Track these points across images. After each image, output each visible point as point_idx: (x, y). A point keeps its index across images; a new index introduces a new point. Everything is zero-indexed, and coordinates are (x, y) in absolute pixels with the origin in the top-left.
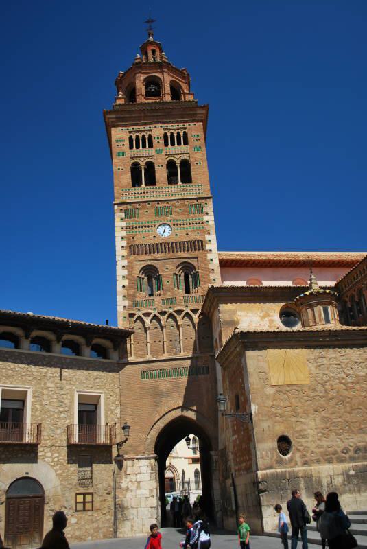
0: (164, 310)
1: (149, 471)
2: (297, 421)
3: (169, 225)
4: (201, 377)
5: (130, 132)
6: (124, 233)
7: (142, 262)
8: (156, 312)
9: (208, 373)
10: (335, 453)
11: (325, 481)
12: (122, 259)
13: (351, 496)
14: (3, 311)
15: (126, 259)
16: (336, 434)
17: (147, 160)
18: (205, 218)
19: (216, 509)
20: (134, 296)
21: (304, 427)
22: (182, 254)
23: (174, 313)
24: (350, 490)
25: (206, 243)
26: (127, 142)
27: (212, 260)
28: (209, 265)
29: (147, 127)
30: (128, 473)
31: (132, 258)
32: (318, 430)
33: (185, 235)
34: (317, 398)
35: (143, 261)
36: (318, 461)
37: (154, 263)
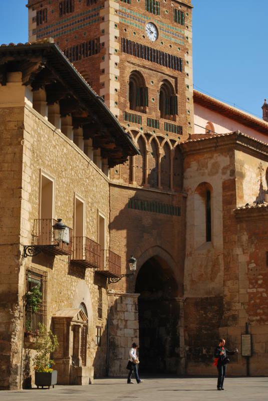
0: (149, 132)
1: (134, 311)
3: (157, 29)
4: (174, 217)
7: (133, 66)
8: (142, 132)
9: (179, 215)
12: (115, 54)
15: (119, 55)
18: (188, 33)
19: (181, 356)
22: (167, 70)
23: (156, 138)
28: (186, 92)
30: (118, 309)
31: (124, 55)
33: (168, 45)
35: (132, 63)
37: (142, 70)
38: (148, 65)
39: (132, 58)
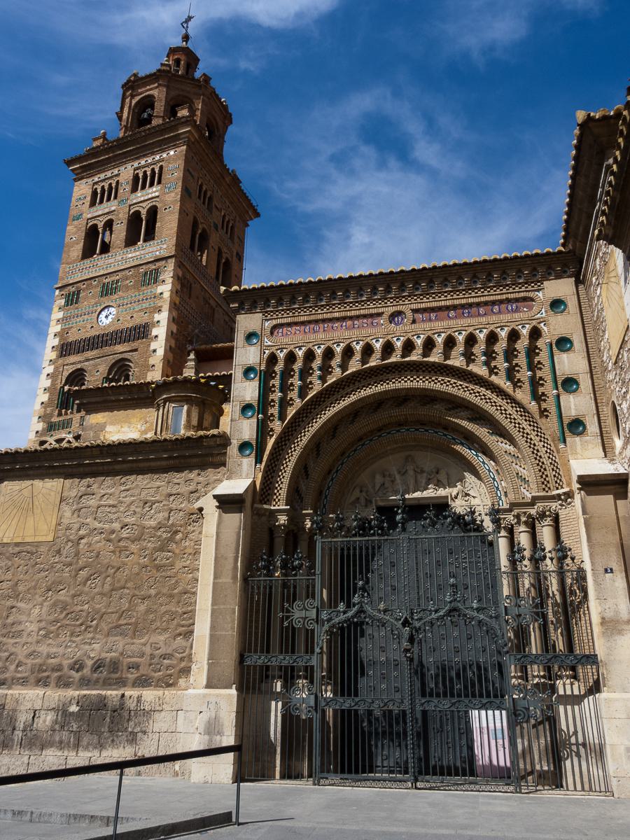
2: (13, 607)
5: (96, 183)
6: (58, 328)
10: (59, 668)
11: (23, 718)
12: (49, 365)
13: (60, 753)
14: (3, 449)
16: (72, 635)
17: (107, 219)
20: (51, 415)
21: (24, 618)
22: (120, 348)
24: (61, 742)
25: (154, 326)
26: (89, 199)
27: (155, 351)
29: (116, 172)
31: (60, 361)
32: (43, 625)
34: (59, 566)
35: (73, 364)
36: (24, 682)
38: (95, 355)
39: (73, 359)
